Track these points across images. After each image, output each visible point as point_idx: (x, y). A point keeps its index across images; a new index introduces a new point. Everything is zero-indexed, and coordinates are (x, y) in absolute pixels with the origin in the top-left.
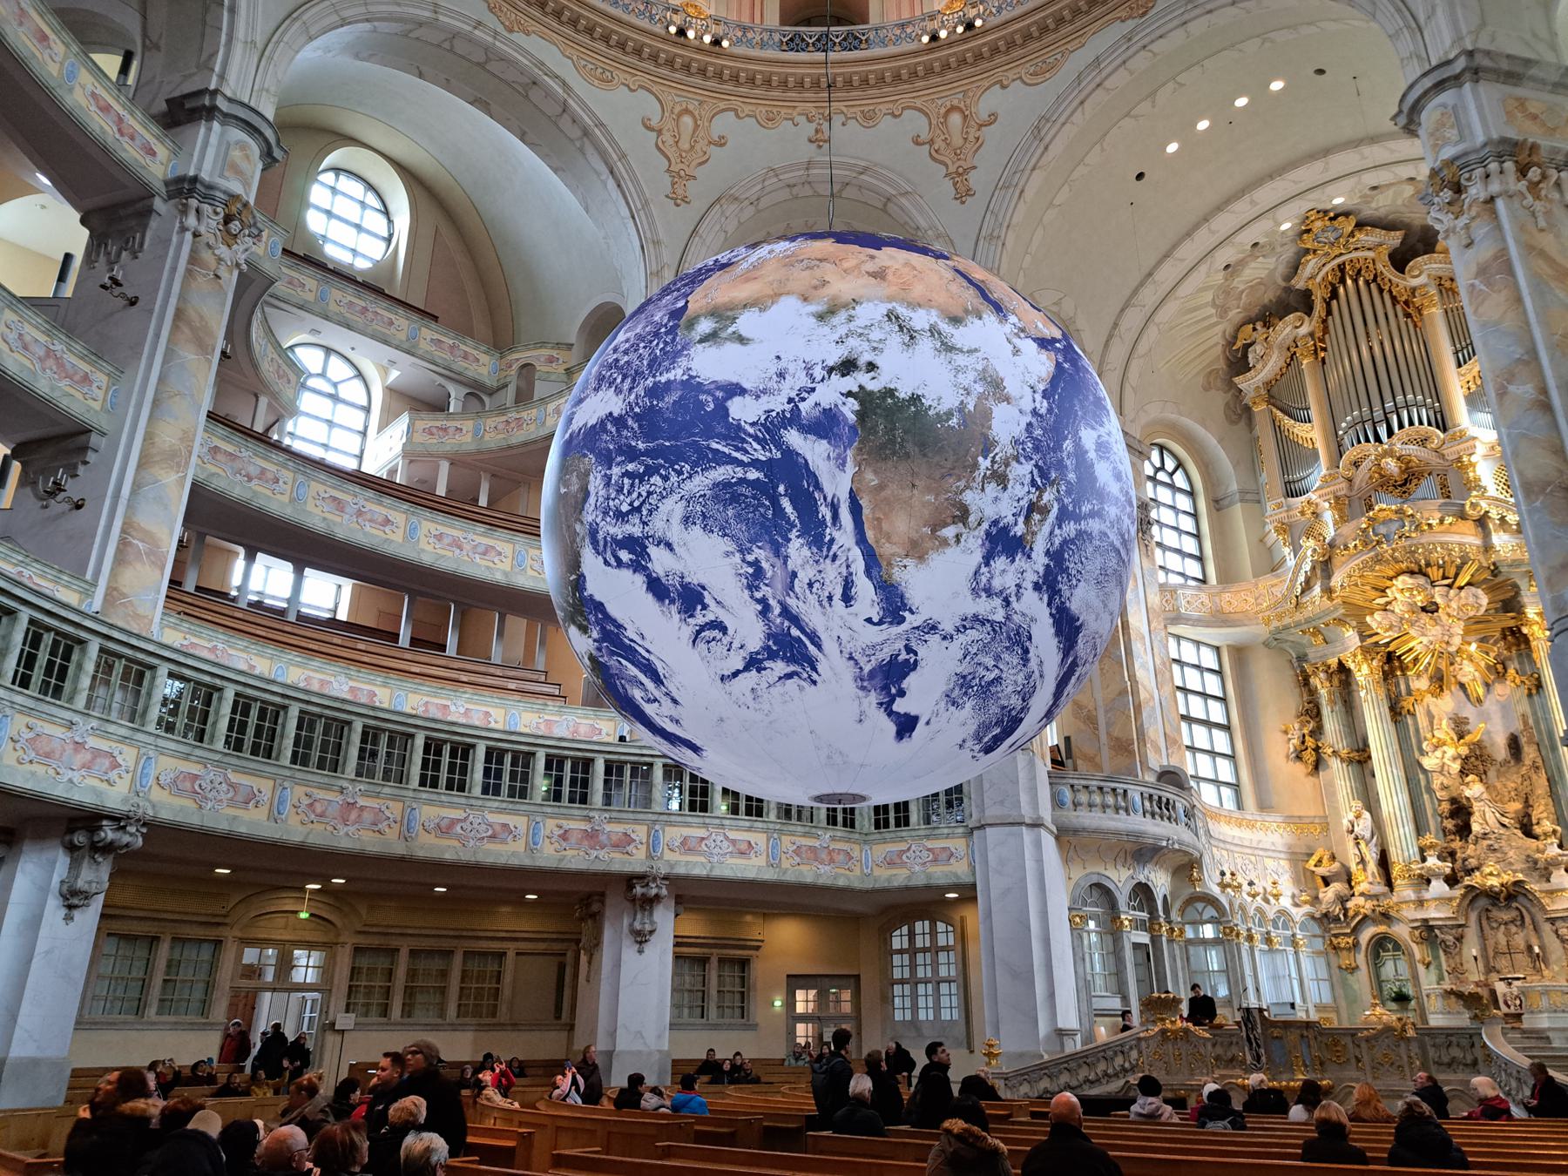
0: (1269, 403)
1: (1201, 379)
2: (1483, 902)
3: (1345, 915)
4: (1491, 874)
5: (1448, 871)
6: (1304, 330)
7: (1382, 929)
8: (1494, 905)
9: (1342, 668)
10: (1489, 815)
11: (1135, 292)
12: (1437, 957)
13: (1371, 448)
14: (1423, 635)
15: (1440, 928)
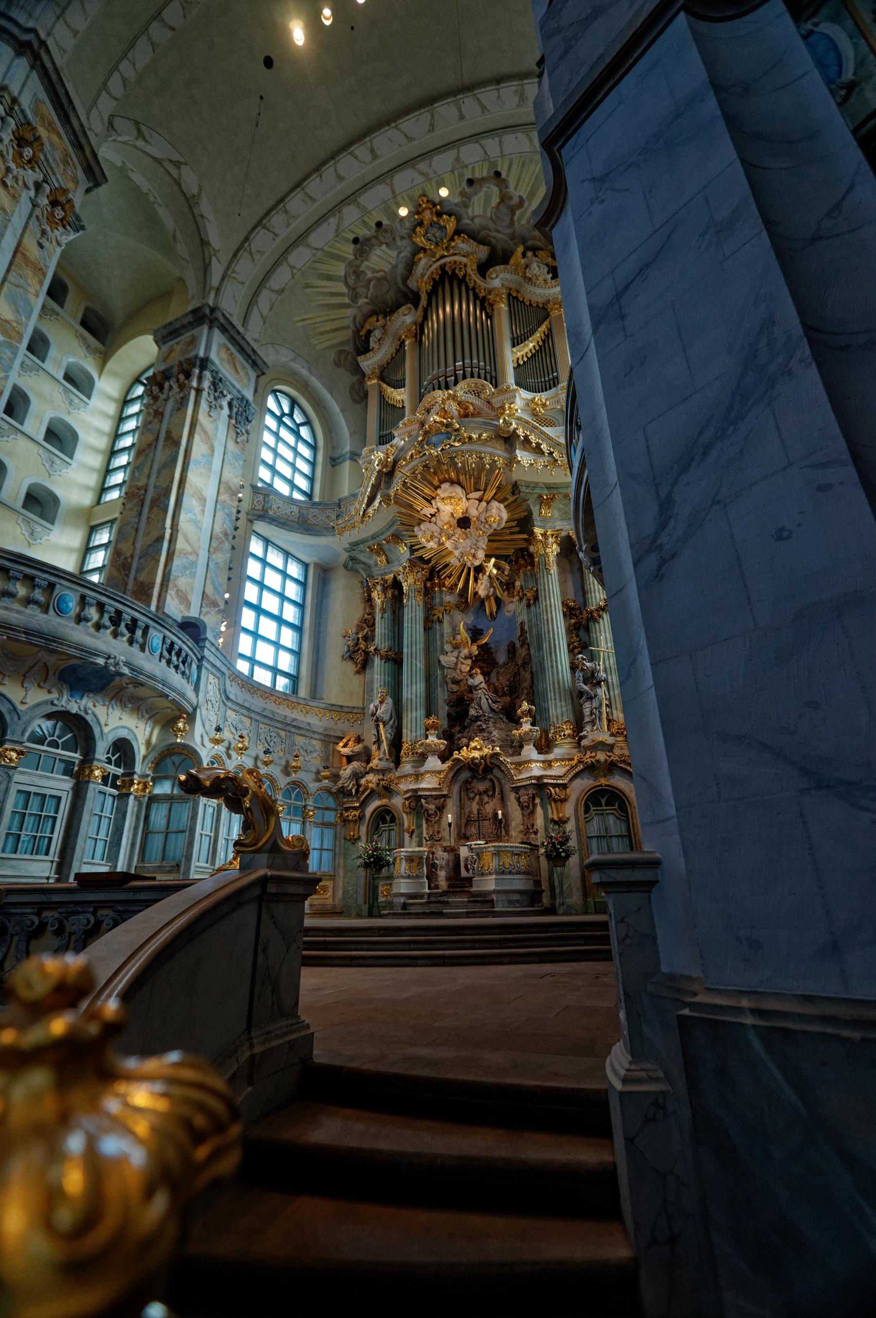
0: (382, 378)
1: (332, 355)
2: (465, 775)
3: (357, 791)
4: (475, 748)
5: (442, 747)
6: (409, 319)
7: (384, 801)
8: (474, 777)
9: (397, 585)
10: (484, 700)
11: (268, 213)
12: (419, 826)
13: (439, 395)
14: (456, 548)
15: (426, 797)
